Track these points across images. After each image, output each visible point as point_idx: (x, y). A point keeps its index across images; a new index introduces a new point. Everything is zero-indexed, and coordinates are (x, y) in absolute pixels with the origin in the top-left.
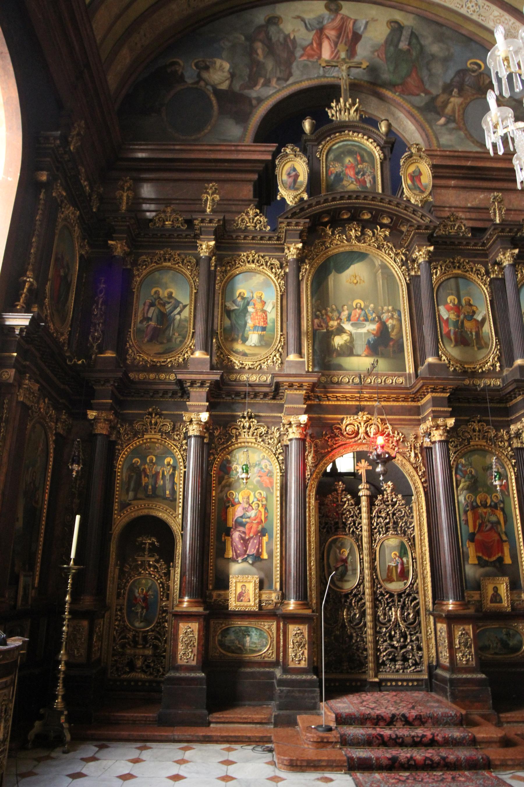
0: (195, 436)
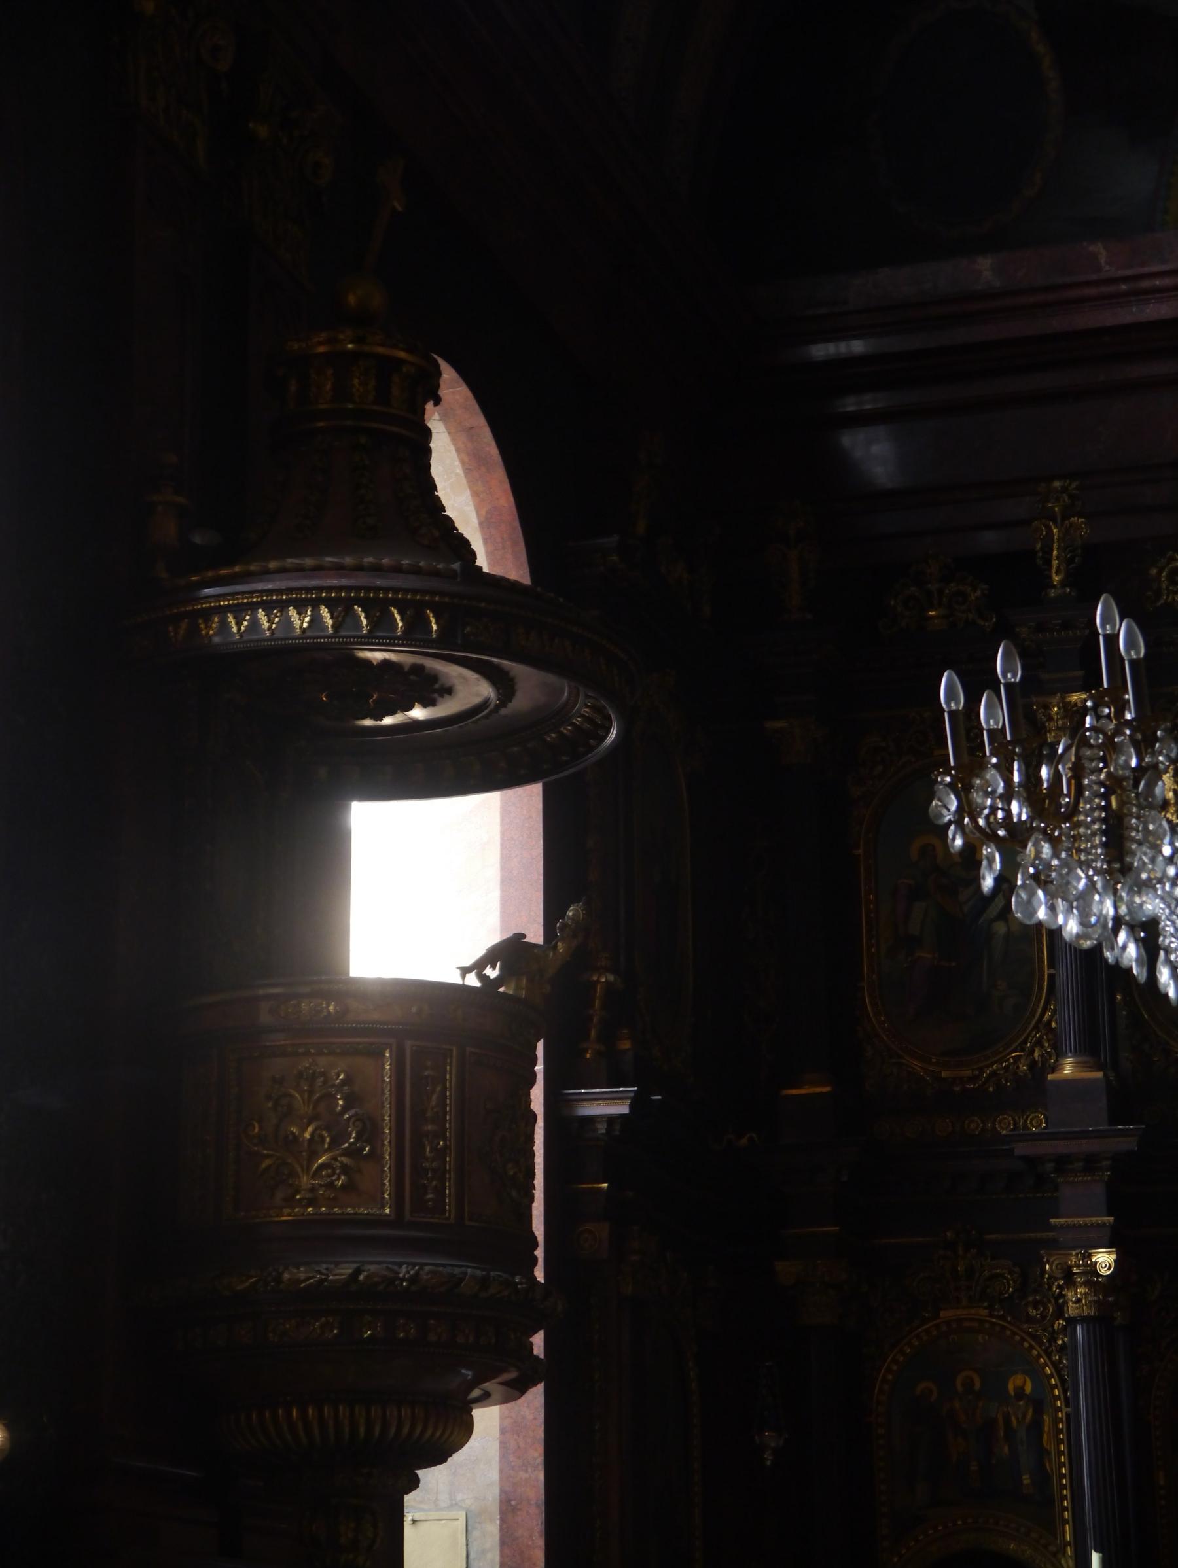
0: (1083, 1320)
